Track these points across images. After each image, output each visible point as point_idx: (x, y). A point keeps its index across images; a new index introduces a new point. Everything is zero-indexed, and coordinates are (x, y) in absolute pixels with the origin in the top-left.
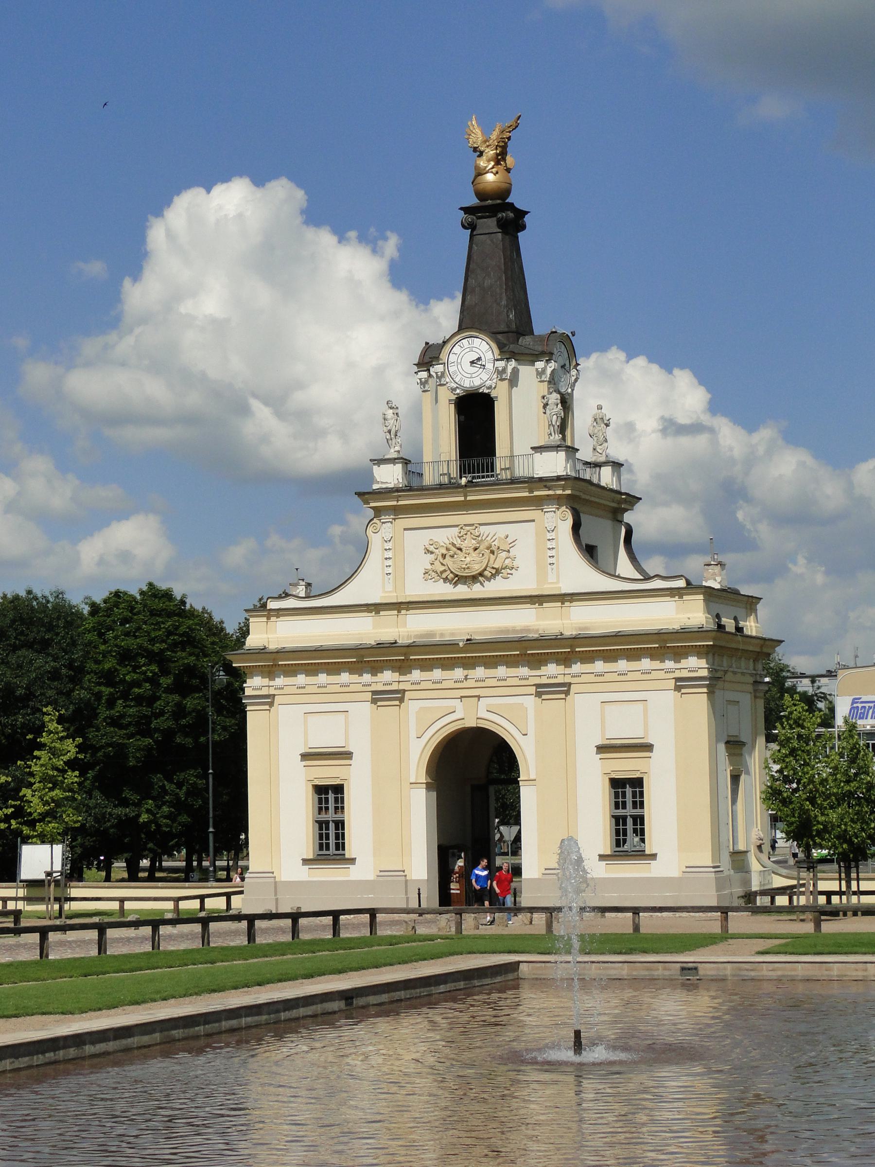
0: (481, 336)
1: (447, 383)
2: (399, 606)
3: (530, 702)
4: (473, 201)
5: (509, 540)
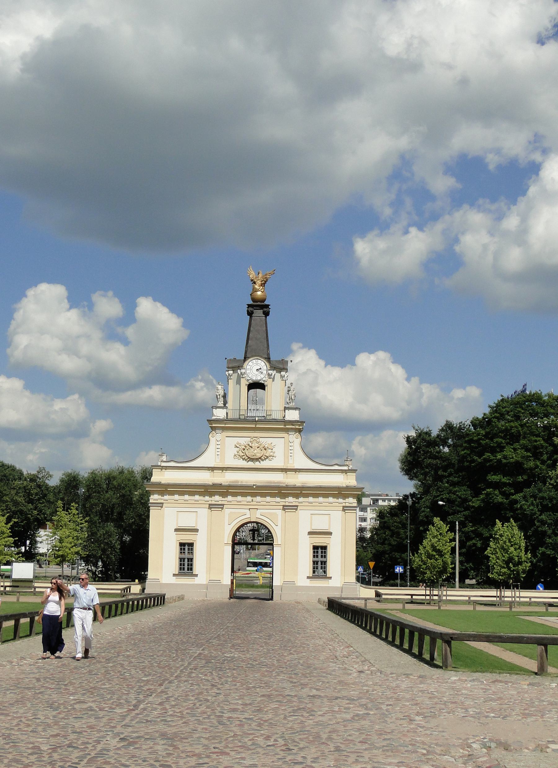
0: (262, 359)
2: (223, 469)
3: (280, 512)
4: (251, 302)
5: (273, 445)
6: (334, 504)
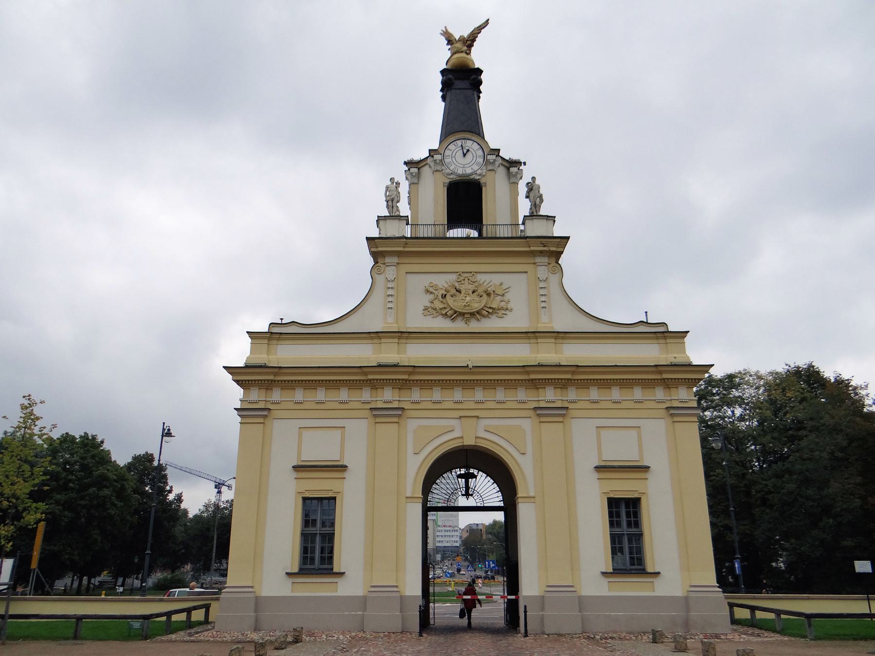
1: (442, 170)
3: (527, 425)
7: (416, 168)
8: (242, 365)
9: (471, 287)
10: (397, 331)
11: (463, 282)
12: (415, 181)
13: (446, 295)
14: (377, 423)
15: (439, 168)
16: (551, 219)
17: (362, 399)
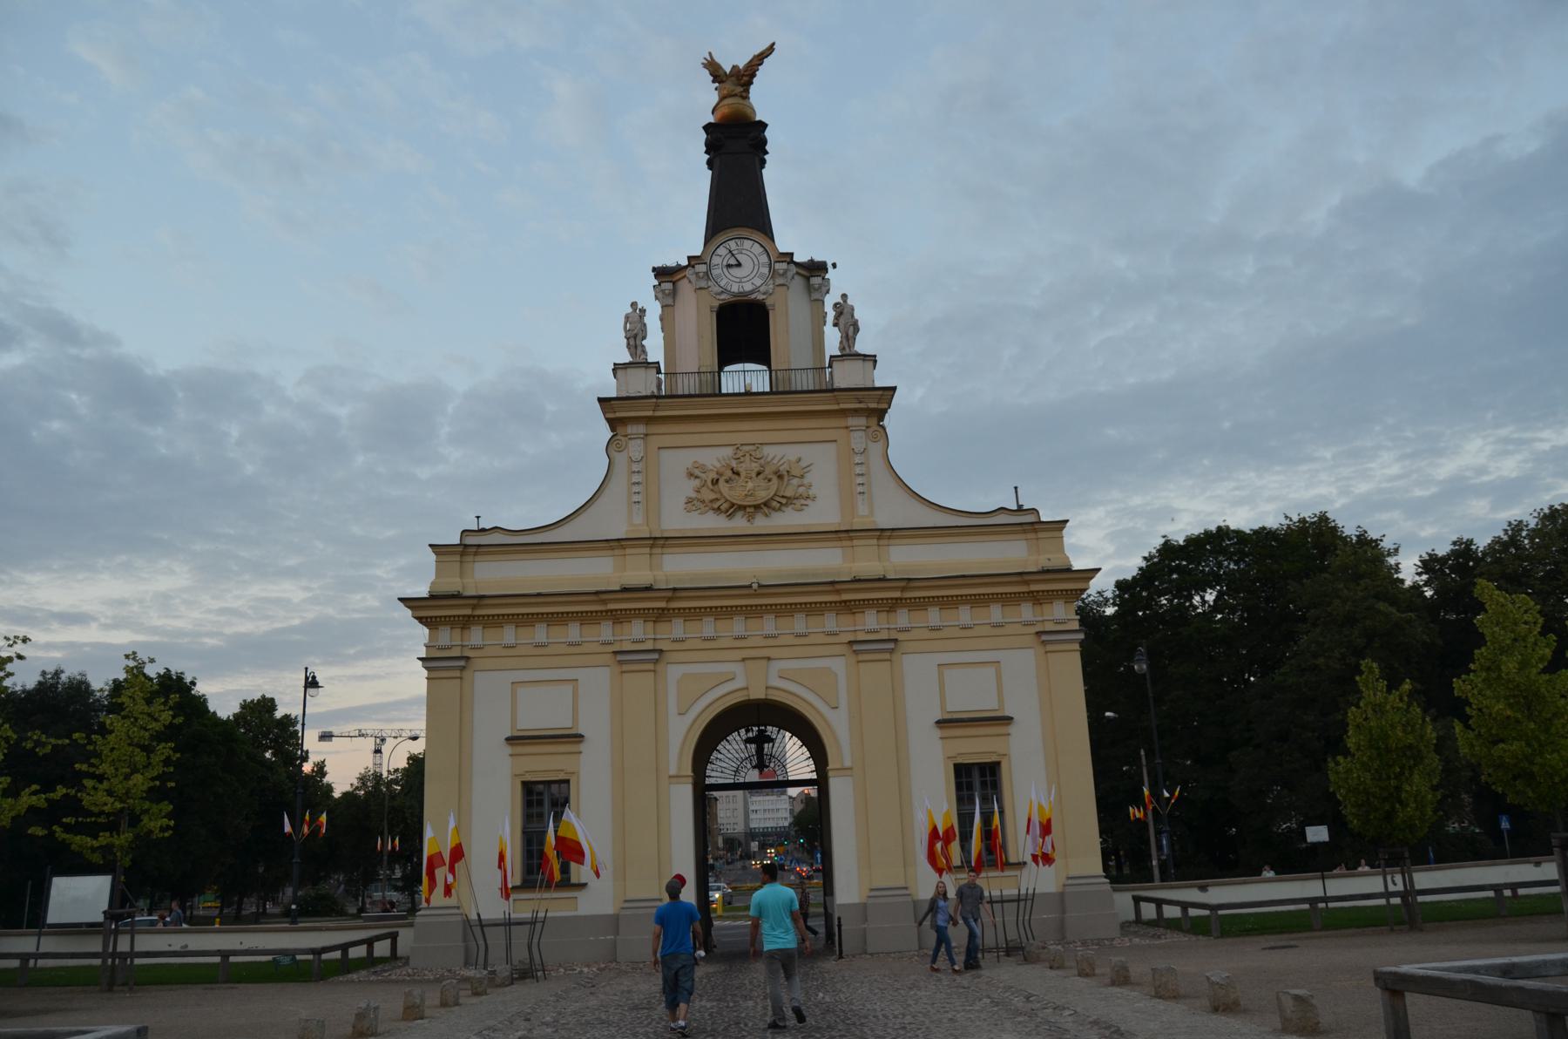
1: (709, 287)
3: (839, 666)
5: (803, 464)
6: (1008, 630)
7: (671, 282)
8: (425, 595)
9: (755, 467)
10: (648, 536)
11: (742, 459)
12: (670, 301)
13: (718, 480)
14: (625, 672)
15: (703, 284)
16: (873, 359)
17: (601, 639)
